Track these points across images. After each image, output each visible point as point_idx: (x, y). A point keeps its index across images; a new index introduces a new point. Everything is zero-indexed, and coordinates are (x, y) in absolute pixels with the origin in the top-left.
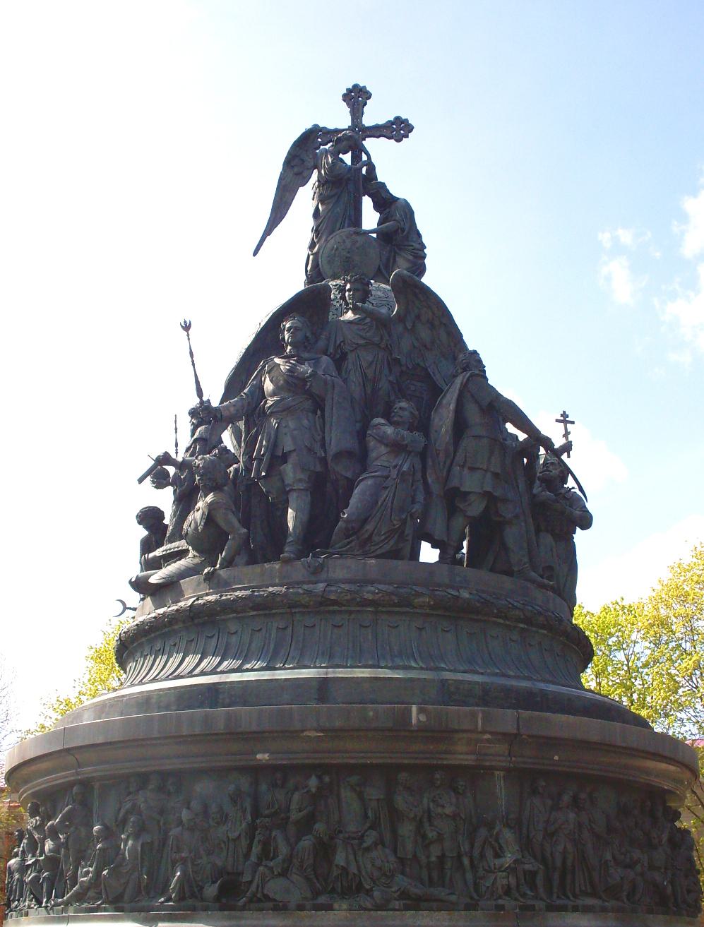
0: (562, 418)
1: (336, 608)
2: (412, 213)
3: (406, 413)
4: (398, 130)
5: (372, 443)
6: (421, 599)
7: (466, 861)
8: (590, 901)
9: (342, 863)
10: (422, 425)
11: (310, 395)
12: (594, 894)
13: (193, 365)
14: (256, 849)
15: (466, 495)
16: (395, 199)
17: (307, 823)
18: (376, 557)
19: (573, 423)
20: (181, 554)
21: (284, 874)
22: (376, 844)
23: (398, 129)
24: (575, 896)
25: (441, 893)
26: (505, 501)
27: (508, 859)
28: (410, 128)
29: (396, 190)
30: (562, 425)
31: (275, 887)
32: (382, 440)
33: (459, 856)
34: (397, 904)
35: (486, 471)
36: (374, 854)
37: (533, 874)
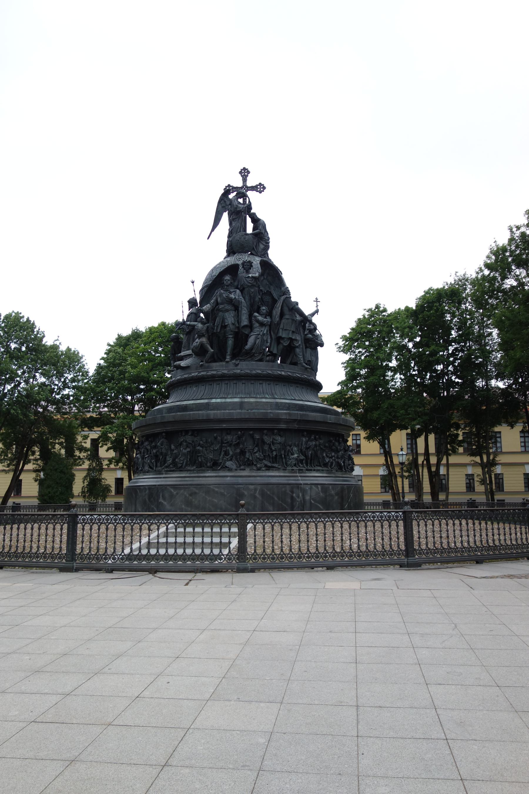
2: (265, 225)
3: (265, 311)
4: (260, 188)
7: (283, 456)
8: (319, 468)
9: (248, 457)
10: (270, 314)
12: (320, 466)
14: (223, 453)
16: (259, 220)
17: (238, 444)
18: (256, 361)
20: (189, 356)
21: (231, 460)
22: (257, 451)
23: (260, 188)
26: (296, 340)
27: (296, 455)
28: (264, 188)
29: (259, 216)
31: (228, 464)
32: (258, 321)
33: (281, 455)
34: (264, 469)
36: (257, 454)
37: (303, 460)
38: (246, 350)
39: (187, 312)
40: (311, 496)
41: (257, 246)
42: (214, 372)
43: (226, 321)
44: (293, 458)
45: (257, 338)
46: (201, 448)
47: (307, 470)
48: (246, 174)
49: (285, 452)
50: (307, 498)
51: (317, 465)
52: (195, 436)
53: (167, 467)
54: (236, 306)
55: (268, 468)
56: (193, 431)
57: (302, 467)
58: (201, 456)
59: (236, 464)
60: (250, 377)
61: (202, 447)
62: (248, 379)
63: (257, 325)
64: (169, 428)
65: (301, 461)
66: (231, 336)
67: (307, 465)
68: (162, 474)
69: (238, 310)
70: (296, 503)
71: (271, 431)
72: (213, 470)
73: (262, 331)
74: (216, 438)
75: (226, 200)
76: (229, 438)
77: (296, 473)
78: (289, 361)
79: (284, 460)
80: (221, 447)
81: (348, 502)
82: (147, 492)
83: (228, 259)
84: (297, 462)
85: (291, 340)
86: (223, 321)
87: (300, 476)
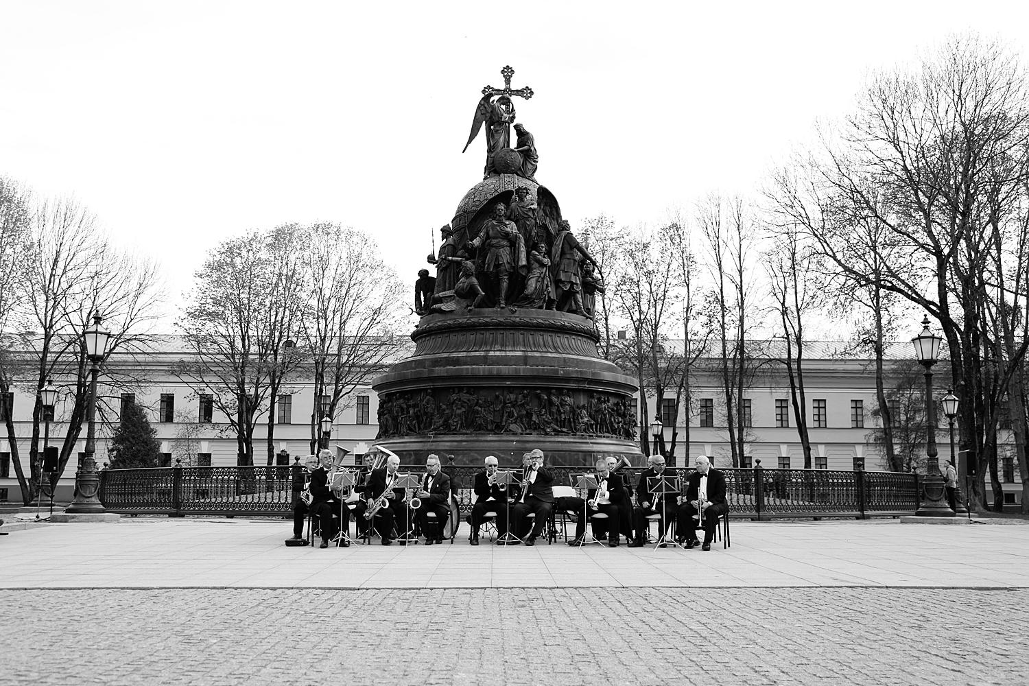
5: (532, 262)
11: (509, 240)
14: (506, 415)
15: (563, 282)
21: (515, 423)
23: (526, 93)
25: (565, 430)
28: (532, 93)
31: (512, 427)
33: (569, 419)
36: (544, 417)
37: (592, 425)
38: (527, 295)
39: (439, 243)
41: (524, 164)
42: (488, 320)
43: (500, 259)
44: (583, 423)
45: (537, 281)
46: (480, 409)
48: (510, 74)
49: (574, 415)
51: (606, 432)
52: (471, 394)
53: (434, 429)
54: (513, 242)
55: (557, 433)
56: (469, 388)
57: (594, 433)
58: (480, 417)
59: (521, 428)
60: (529, 326)
61: (481, 407)
62: (526, 329)
63: (536, 265)
64: (439, 384)
66: (506, 277)
67: (597, 432)
68: (430, 437)
69: (515, 246)
71: (560, 391)
72: (494, 434)
73: (542, 273)
74: (497, 397)
75: (486, 105)
76: (512, 396)
77: (586, 438)
78: (566, 309)
79: (573, 425)
80: (503, 408)
82: (413, 457)
83: (489, 181)
85: (572, 284)
86: (497, 259)
87: (591, 443)
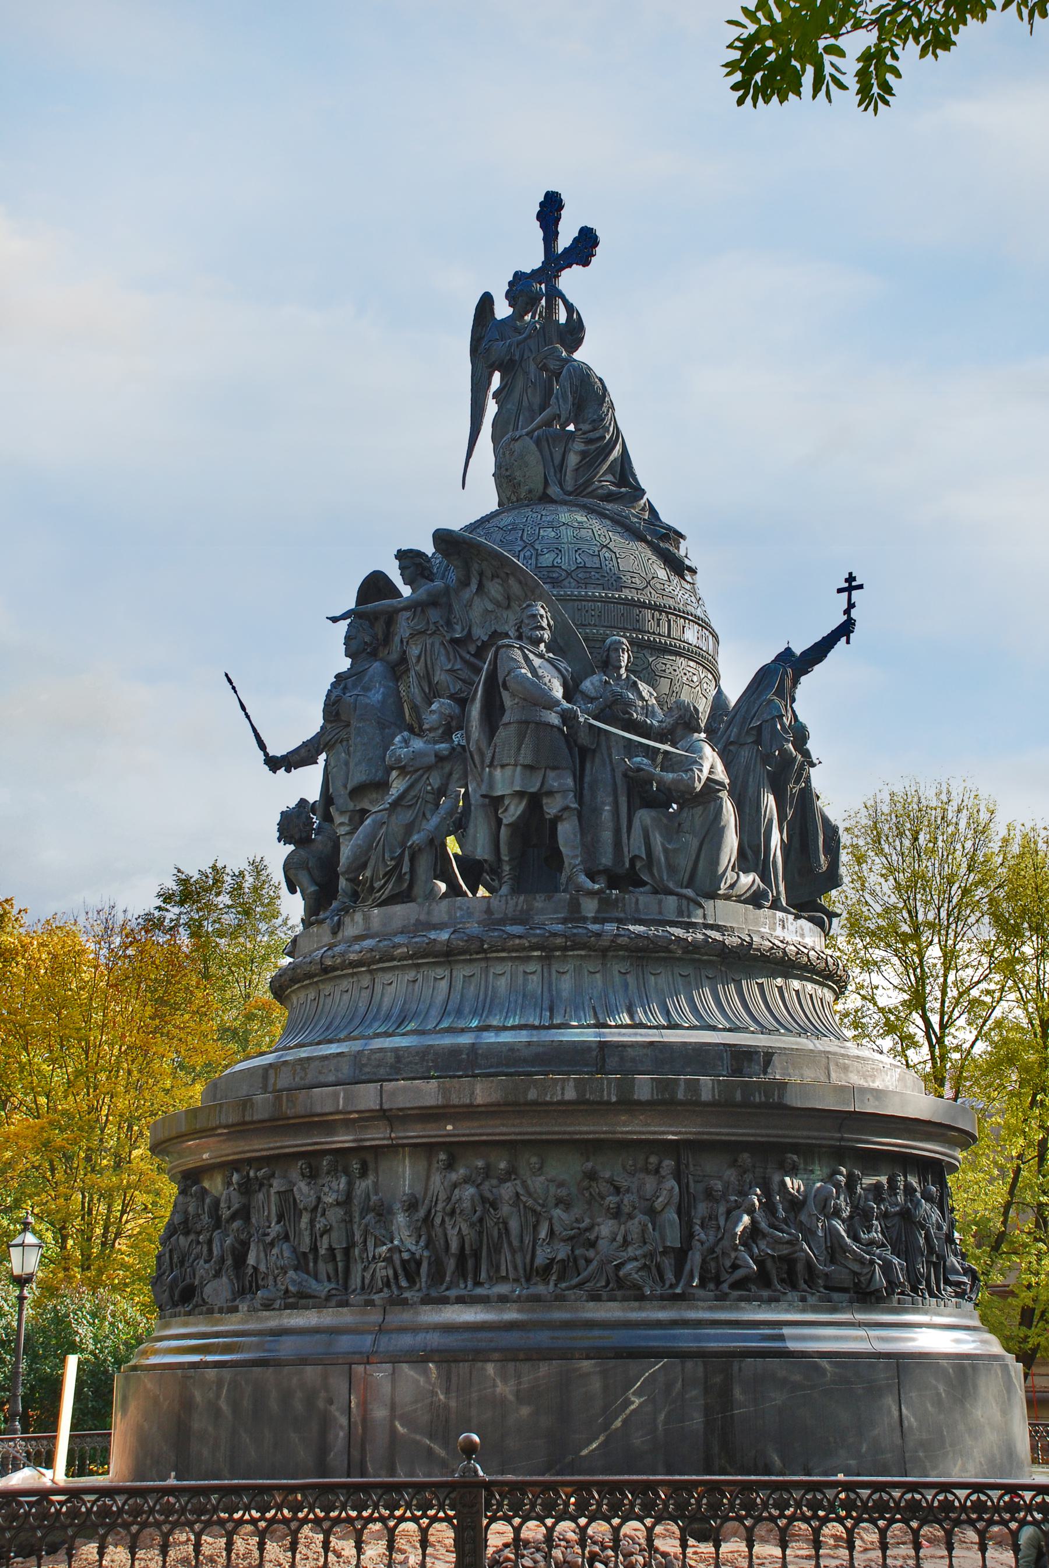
0: (847, 585)
1: (339, 973)
6: (399, 951)
13: (248, 717)
18: (379, 905)
19: (861, 587)
21: (217, 1275)
24: (477, 1284)
30: (846, 594)
35: (516, 765)
40: (393, 1407)
47: (427, 1300)
50: (380, 1413)
65: (410, 1269)
70: (337, 1436)
81: (606, 1426)
84: (391, 1272)
